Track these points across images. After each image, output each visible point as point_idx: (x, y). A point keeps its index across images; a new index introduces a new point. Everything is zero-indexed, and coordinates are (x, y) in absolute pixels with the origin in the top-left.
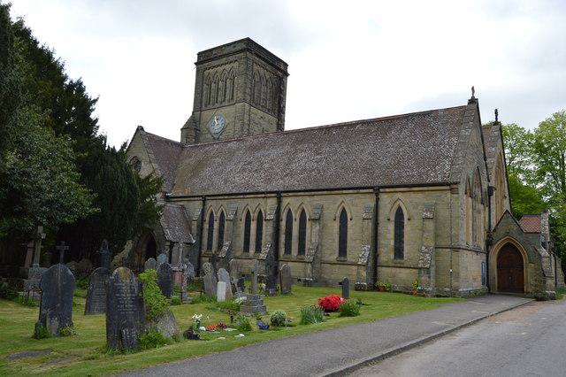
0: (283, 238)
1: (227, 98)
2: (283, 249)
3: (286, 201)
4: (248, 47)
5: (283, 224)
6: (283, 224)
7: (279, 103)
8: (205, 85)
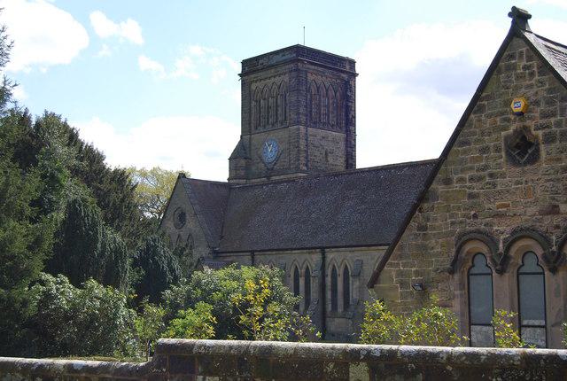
0: (329, 295)
1: (280, 119)
2: (330, 305)
3: (330, 256)
4: (299, 54)
5: (329, 280)
6: (329, 280)
7: (347, 115)
8: (253, 103)
